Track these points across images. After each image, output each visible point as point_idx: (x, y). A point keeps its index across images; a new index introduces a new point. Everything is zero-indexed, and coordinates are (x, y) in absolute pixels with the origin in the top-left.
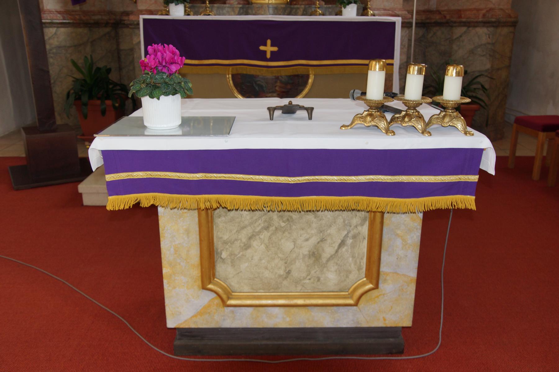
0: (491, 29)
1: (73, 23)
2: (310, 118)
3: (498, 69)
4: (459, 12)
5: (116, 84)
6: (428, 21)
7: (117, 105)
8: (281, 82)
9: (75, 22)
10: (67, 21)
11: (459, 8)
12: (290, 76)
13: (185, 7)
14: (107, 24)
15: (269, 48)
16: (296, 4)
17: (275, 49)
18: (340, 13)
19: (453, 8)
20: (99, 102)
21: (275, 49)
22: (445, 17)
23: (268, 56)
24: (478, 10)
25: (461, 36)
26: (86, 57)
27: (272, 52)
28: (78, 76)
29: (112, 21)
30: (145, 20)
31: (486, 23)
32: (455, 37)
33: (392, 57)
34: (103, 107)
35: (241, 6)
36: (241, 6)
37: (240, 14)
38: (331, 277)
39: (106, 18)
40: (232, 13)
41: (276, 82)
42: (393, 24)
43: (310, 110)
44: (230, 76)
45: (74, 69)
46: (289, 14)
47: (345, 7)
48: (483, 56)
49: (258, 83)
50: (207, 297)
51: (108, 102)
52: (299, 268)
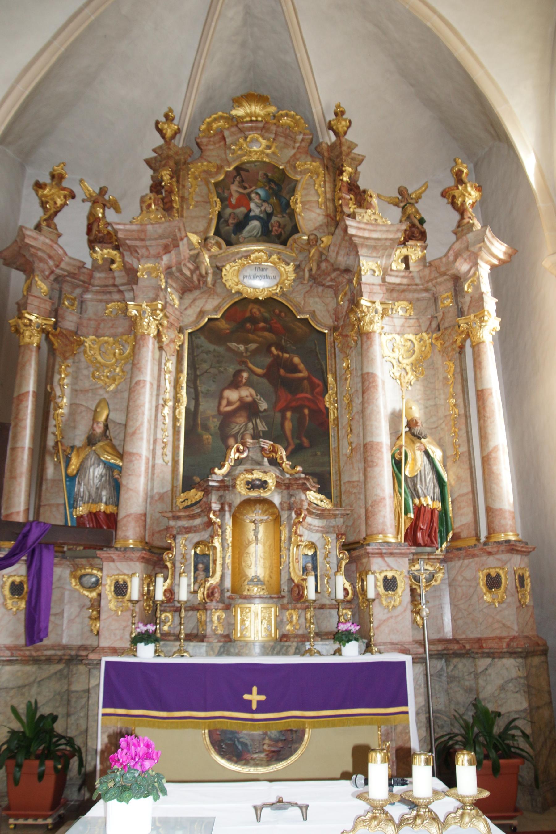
0: (520, 660)
1: (22, 660)
2: (305, 818)
3: (538, 708)
4: (479, 640)
5: (61, 737)
6: (445, 652)
7: (60, 766)
8: (271, 739)
9: (24, 658)
10: (15, 658)
11: (479, 636)
12: (281, 731)
13: (156, 646)
14: (60, 661)
15: (254, 697)
16: (286, 641)
17: (263, 698)
18: (338, 652)
19: (472, 636)
20: (37, 762)
21: (263, 698)
22: (465, 647)
23: (254, 707)
24: (501, 639)
25: (486, 669)
26: (29, 702)
27: (259, 702)
28: (16, 726)
29: (66, 657)
30: (107, 663)
31: (512, 654)
32: (480, 670)
33: (406, 704)
34: (42, 768)
35: (221, 644)
36: (221, 644)
37: (220, 654)
39: (60, 653)
40: (211, 653)
41: (264, 739)
42: (403, 664)
43: (304, 809)
44: (207, 731)
45: (12, 716)
46: (278, 654)
47: (344, 646)
48: (517, 692)
49: (241, 740)
51: (49, 763)
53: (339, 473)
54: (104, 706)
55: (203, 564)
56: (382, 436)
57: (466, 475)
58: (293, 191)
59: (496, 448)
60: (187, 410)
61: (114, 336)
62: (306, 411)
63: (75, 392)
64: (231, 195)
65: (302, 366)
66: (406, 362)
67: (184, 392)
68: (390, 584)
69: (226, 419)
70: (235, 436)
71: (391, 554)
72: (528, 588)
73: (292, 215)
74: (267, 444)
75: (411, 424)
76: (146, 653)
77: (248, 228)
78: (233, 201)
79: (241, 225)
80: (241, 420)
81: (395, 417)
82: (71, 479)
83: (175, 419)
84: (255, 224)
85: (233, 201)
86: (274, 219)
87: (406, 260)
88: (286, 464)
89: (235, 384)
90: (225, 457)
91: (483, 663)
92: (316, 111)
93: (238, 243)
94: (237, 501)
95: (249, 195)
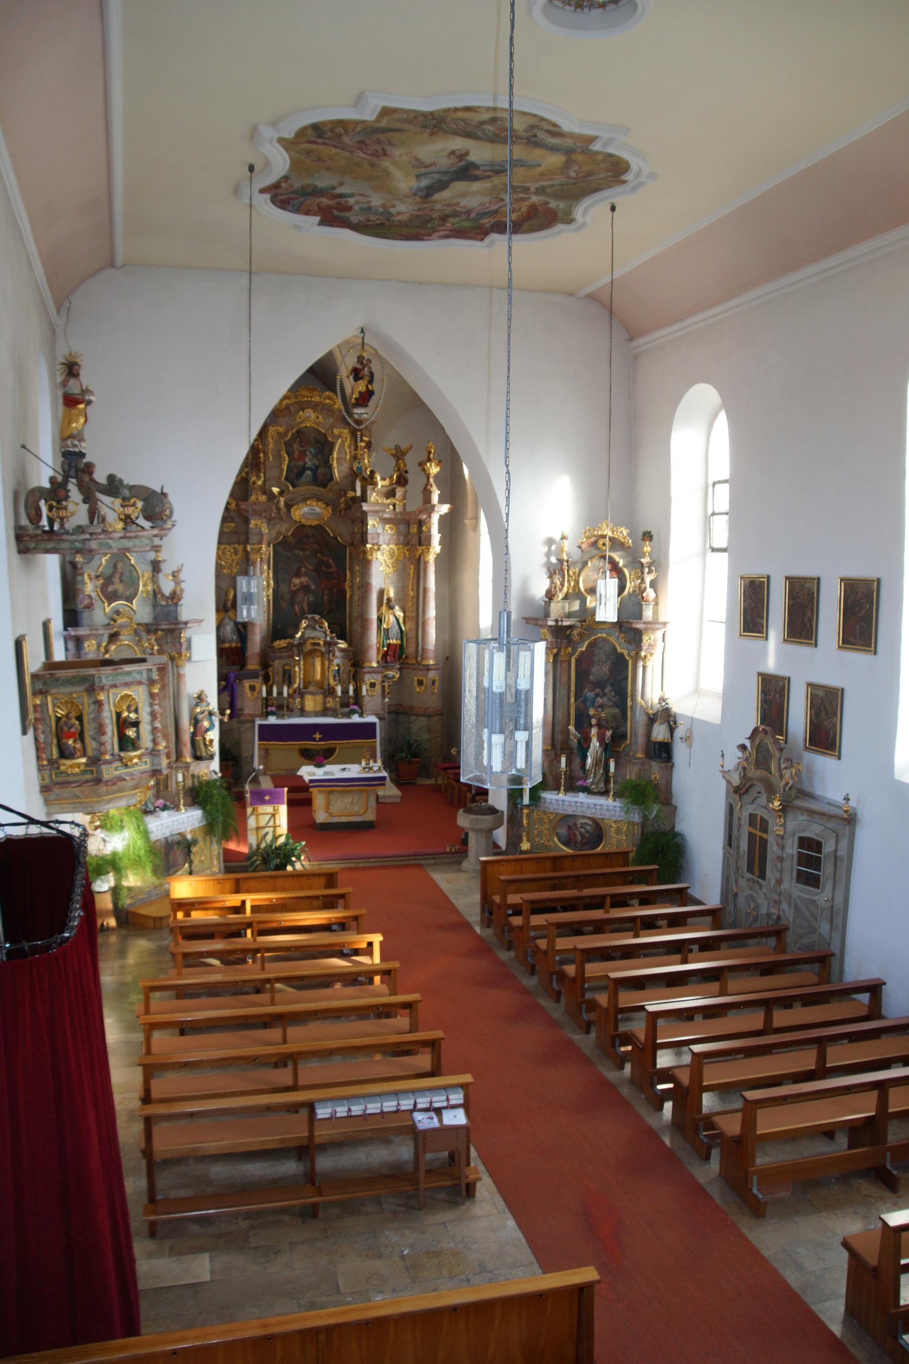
15: (317, 736)
30: (260, 726)
31: (425, 716)
33: (375, 737)
38: (356, 808)
50: (327, 815)
52: (348, 806)
53: (351, 624)
54: (260, 740)
55: (288, 678)
56: (374, 616)
57: (414, 627)
58: (331, 453)
59: (428, 619)
60: (274, 590)
61: (230, 544)
62: (335, 590)
64: (294, 452)
65: (333, 565)
66: (389, 562)
67: (272, 582)
68: (373, 685)
69: (294, 594)
70: (298, 604)
71: (374, 672)
72: (437, 685)
73: (330, 467)
74: (317, 617)
75: (389, 600)
76: (272, 720)
77: (304, 476)
78: (296, 456)
79: (300, 474)
80: (301, 595)
81: (381, 593)
83: (268, 596)
84: (309, 472)
85: (296, 456)
86: (320, 470)
87: (394, 506)
88: (328, 632)
89: (298, 575)
91: (414, 718)
93: (299, 486)
94: (306, 650)
95: (305, 451)
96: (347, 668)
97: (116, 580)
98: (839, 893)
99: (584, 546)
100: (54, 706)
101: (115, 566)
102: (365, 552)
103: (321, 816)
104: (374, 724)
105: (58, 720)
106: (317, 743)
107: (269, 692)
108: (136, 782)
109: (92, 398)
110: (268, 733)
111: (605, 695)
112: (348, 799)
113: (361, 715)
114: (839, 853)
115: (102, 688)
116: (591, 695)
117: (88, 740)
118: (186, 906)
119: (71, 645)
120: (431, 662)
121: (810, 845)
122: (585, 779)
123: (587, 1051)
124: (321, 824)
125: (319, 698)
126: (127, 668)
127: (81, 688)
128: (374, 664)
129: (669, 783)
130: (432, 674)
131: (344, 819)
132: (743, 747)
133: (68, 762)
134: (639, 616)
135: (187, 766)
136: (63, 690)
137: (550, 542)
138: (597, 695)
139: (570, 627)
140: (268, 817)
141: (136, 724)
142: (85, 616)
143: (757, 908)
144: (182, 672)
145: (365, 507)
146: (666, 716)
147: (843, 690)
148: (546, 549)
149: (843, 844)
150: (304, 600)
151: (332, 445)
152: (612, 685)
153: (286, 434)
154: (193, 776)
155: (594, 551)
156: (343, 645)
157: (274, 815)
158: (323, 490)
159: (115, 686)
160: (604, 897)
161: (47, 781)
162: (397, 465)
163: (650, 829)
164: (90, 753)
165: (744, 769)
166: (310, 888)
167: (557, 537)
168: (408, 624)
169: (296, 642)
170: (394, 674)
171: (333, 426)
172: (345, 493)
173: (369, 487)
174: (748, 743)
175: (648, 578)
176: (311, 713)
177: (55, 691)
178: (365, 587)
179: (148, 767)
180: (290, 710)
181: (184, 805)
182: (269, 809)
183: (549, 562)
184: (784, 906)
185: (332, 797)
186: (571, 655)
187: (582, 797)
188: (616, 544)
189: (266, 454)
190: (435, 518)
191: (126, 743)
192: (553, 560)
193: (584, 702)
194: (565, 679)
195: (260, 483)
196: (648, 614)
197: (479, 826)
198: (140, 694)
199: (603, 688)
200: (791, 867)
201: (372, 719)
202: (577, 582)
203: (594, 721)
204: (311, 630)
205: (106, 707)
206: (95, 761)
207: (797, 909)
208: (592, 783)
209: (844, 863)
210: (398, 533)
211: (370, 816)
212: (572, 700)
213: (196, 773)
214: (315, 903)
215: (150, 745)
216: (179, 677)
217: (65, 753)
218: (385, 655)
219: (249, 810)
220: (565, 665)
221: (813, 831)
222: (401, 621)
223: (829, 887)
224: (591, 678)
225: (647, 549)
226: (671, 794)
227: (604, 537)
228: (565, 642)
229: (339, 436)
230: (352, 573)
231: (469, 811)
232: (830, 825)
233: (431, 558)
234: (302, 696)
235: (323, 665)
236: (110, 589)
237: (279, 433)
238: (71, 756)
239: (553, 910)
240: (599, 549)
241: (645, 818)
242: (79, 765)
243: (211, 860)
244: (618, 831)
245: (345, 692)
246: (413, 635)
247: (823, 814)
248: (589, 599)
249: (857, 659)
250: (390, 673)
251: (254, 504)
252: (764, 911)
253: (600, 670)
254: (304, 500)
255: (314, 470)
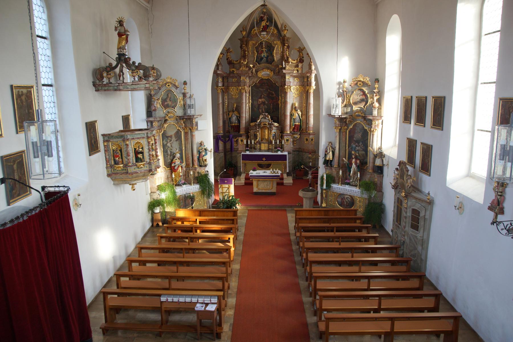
15: (264, 159)
53: (281, 116)
55: (256, 137)
56: (288, 113)
58: (273, 51)
63: (228, 99)
68: (287, 140)
69: (259, 105)
74: (267, 114)
75: (296, 107)
76: (248, 153)
81: (293, 105)
82: (230, 119)
87: (298, 70)
89: (261, 98)
90: (259, 118)
92: (279, 26)
96: (278, 134)
97: (168, 100)
98: (426, 233)
99: (352, 85)
100: (112, 146)
101: (168, 95)
102: (285, 89)
103: (255, 190)
104: (286, 155)
105: (113, 150)
106: (264, 162)
107: (247, 142)
108: (143, 174)
109: (128, 33)
110: (246, 158)
111: (359, 146)
112: (266, 183)
113: (282, 152)
114: (426, 217)
115: (128, 140)
116: (354, 146)
117: (124, 158)
118: (182, 220)
119: (149, 124)
120: (311, 132)
121: (416, 213)
122: (350, 180)
123: (302, 288)
124: (255, 192)
125: (267, 145)
126: (137, 132)
127: (121, 140)
128: (288, 132)
129: (381, 183)
130: (311, 137)
131: (264, 191)
132: (397, 169)
133: (116, 166)
134: (371, 114)
135: (196, 169)
136: (115, 140)
137: (340, 83)
138: (357, 146)
139: (345, 118)
140: (226, 189)
141: (142, 153)
142: (153, 113)
143: (397, 237)
144: (194, 134)
145: (284, 71)
146: (381, 155)
147: (432, 146)
148: (338, 86)
149: (428, 213)
150: (263, 107)
151: (274, 47)
152: (362, 142)
153: (256, 44)
154: (198, 173)
155: (356, 87)
156: (276, 124)
157: (228, 188)
158: (270, 65)
159: (133, 139)
160: (333, 227)
161: (110, 172)
162: (300, 55)
163: (372, 201)
164: (125, 163)
165: (397, 178)
166: (227, 216)
167: (342, 81)
168: (303, 117)
169: (257, 124)
170: (297, 136)
171: (274, 40)
172: (278, 66)
173: (287, 64)
174: (398, 167)
175: (375, 98)
176: (264, 151)
177: (112, 140)
178: (285, 103)
179: (148, 169)
180: (255, 149)
181: (193, 183)
182: (227, 186)
183: (339, 91)
184: (406, 237)
185: (259, 182)
186: (347, 129)
187: (347, 187)
188: (364, 84)
189: (248, 52)
190: (313, 76)
191: (138, 160)
192: (341, 91)
193: (352, 148)
194: (344, 139)
195: (245, 63)
196: (375, 113)
197: (306, 196)
198: (144, 142)
199: (359, 143)
200: (409, 221)
201: (286, 153)
202: (350, 100)
203: (353, 156)
204: (265, 119)
205: (130, 146)
206: (126, 166)
207: (410, 239)
208: (352, 182)
209: (428, 221)
210: (300, 82)
211: (274, 190)
212: (347, 147)
213: (200, 171)
214: (229, 222)
215: (148, 161)
216: (192, 136)
217: (116, 163)
218: (294, 129)
219: (219, 186)
220: (344, 133)
221: (417, 206)
222: (300, 115)
223: (422, 231)
224: (354, 139)
225: (377, 86)
226: (382, 187)
227: (360, 81)
228: (344, 124)
229: (277, 44)
230: (281, 97)
231: (303, 190)
232: (423, 204)
233: (312, 91)
234: (260, 144)
235: (268, 132)
236: (166, 103)
237: (253, 44)
238: (118, 164)
239: (323, 231)
240: (358, 86)
241: (370, 197)
242: (120, 167)
243: (204, 203)
244: (360, 201)
245: (276, 143)
246: (305, 121)
247: (420, 200)
248: (354, 107)
249: (437, 132)
250: (296, 136)
251: (242, 71)
252: (399, 238)
253: (358, 136)
254: (263, 69)
255: (267, 58)
